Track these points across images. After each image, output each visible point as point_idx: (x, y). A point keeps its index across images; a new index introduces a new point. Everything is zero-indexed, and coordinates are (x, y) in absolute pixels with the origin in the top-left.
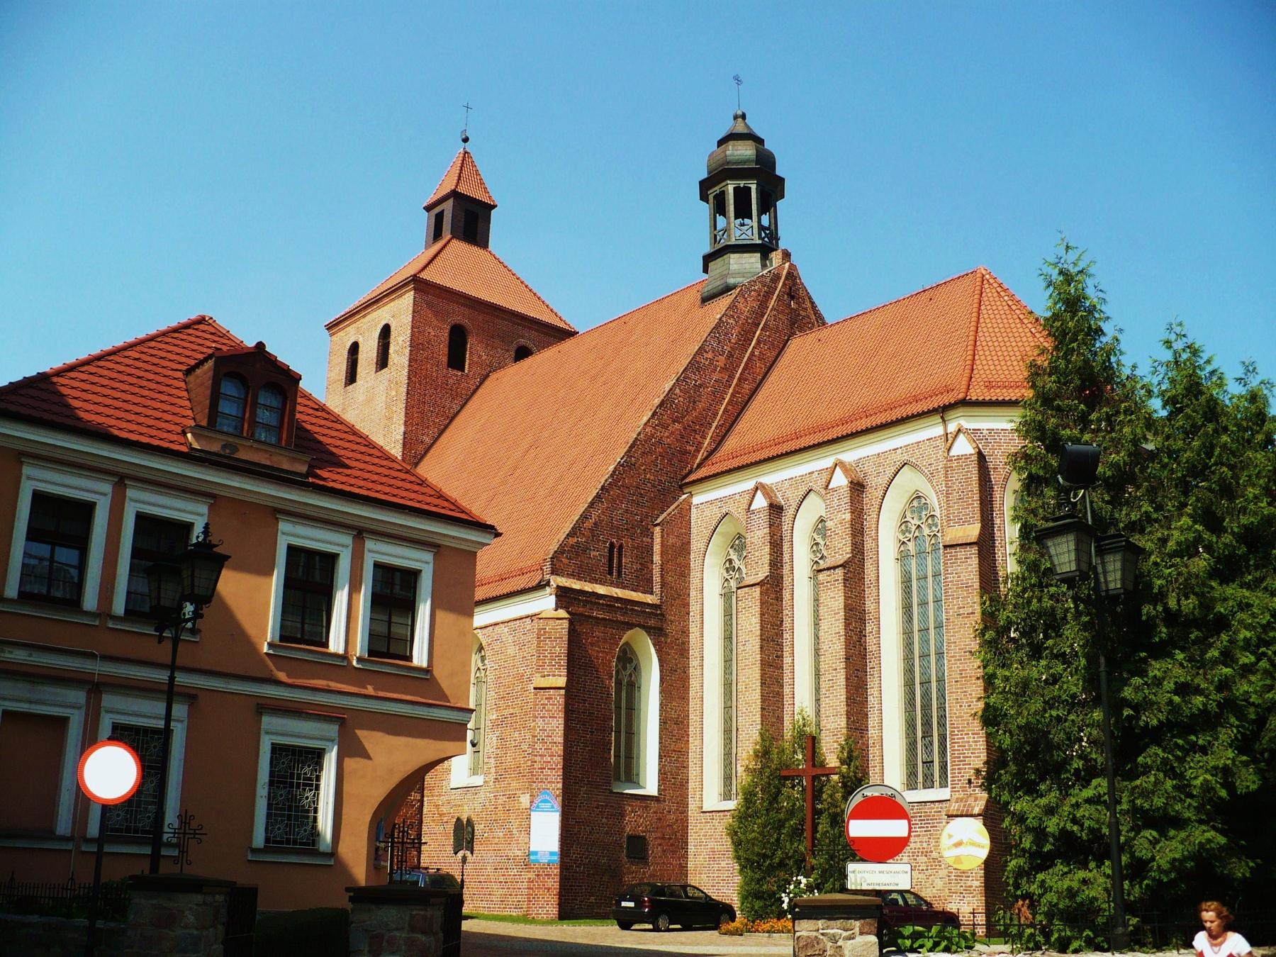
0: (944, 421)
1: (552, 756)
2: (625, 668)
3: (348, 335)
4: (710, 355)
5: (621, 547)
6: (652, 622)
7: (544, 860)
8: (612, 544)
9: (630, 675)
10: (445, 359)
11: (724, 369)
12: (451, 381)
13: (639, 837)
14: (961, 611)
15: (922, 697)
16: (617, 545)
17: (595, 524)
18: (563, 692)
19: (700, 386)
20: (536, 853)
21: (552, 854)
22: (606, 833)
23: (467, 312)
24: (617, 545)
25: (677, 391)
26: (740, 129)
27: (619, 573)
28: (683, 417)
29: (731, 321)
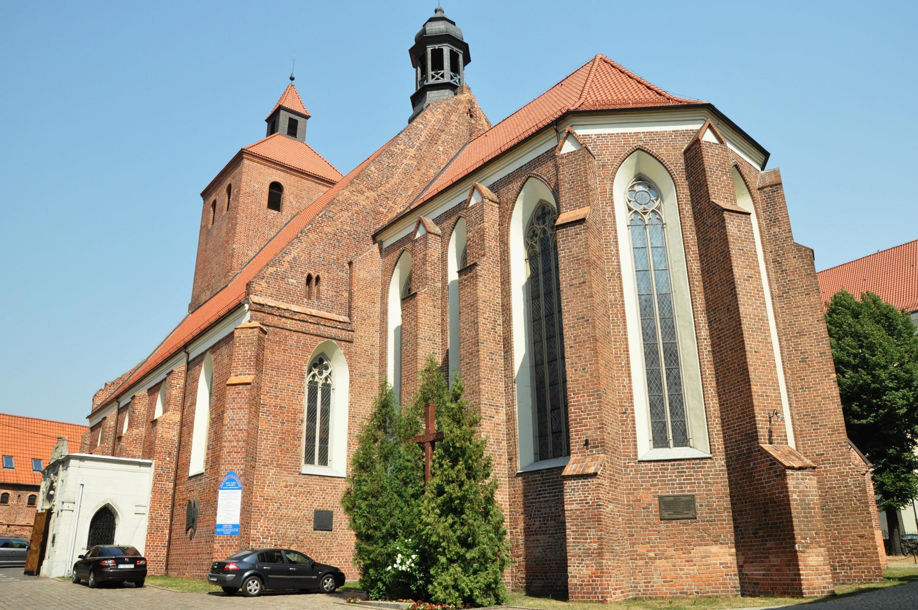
0: (557, 131)
1: (238, 441)
2: (321, 373)
3: (211, 199)
4: (402, 147)
5: (318, 279)
6: (343, 334)
7: (228, 532)
8: (309, 278)
9: (326, 379)
10: (265, 203)
11: (415, 157)
12: (269, 217)
13: (327, 512)
14: (574, 282)
15: (550, 375)
16: (314, 277)
17: (294, 258)
18: (249, 387)
19: (393, 167)
20: (221, 526)
21: (234, 526)
22: (295, 508)
23: (283, 174)
24: (314, 277)
25: (373, 168)
26: (439, 15)
27: (318, 298)
28: (377, 187)
29: (421, 126)
